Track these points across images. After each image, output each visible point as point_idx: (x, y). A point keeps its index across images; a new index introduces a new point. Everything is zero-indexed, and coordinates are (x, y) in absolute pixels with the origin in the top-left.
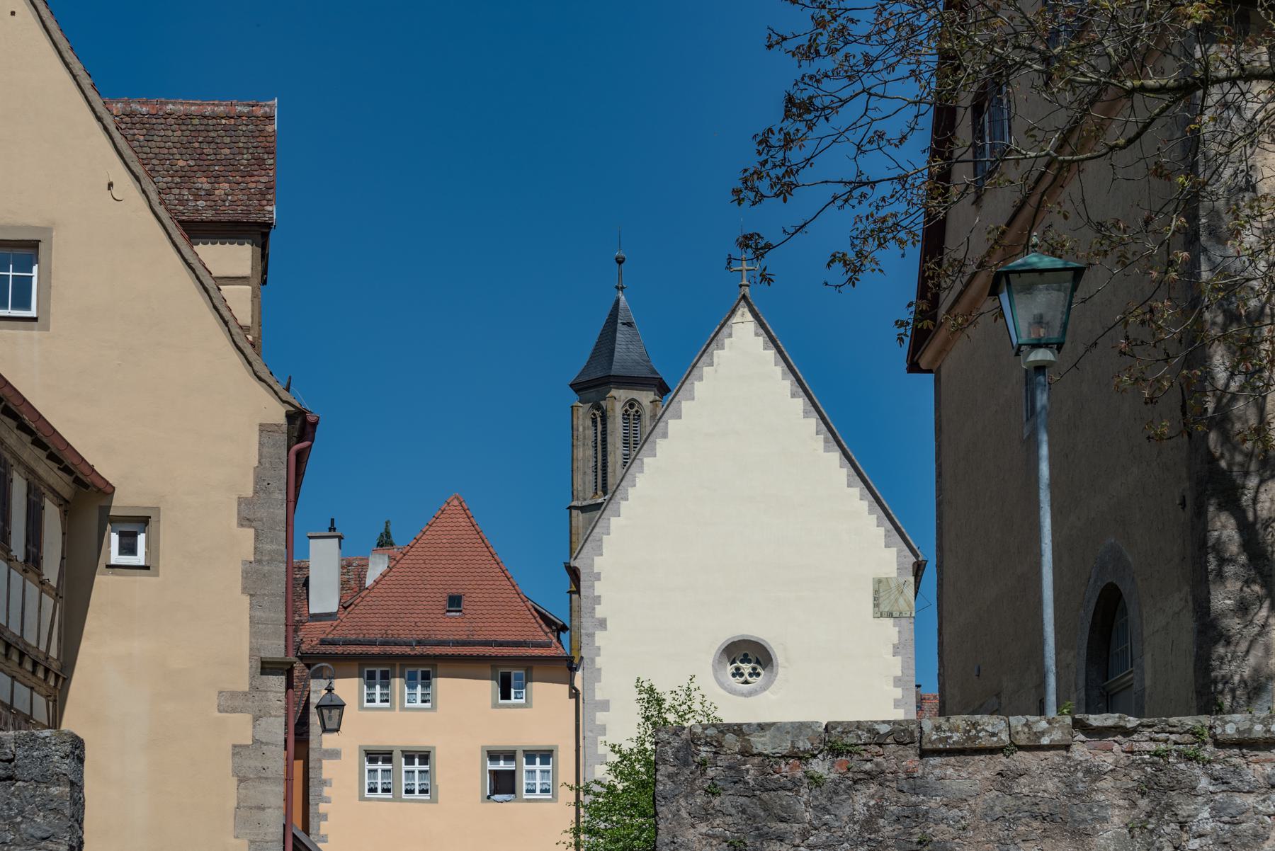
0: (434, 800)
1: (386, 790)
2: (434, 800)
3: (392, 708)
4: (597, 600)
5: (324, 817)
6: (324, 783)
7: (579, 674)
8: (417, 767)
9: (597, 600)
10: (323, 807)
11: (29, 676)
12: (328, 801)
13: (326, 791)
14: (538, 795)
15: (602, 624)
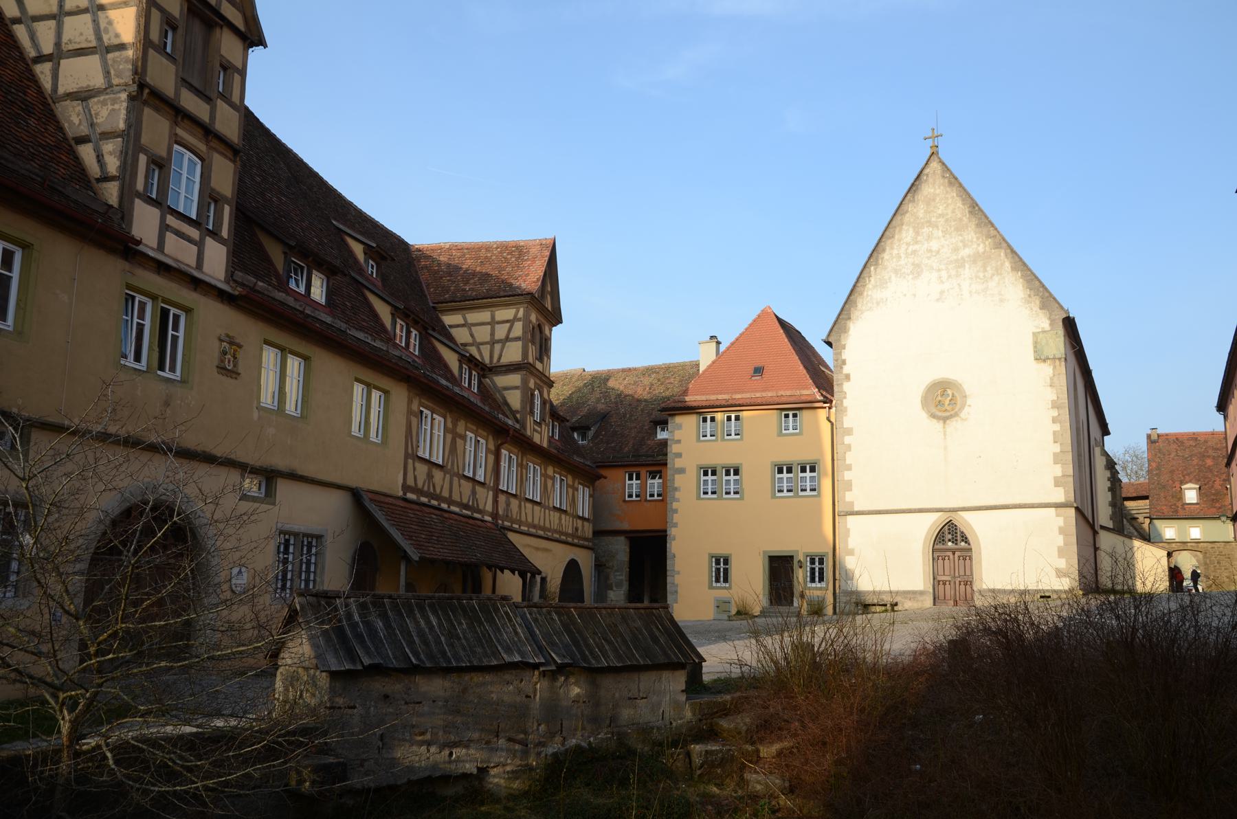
0: (742, 498)
1: (713, 493)
2: (742, 498)
6: (676, 489)
8: (732, 477)
12: (678, 500)
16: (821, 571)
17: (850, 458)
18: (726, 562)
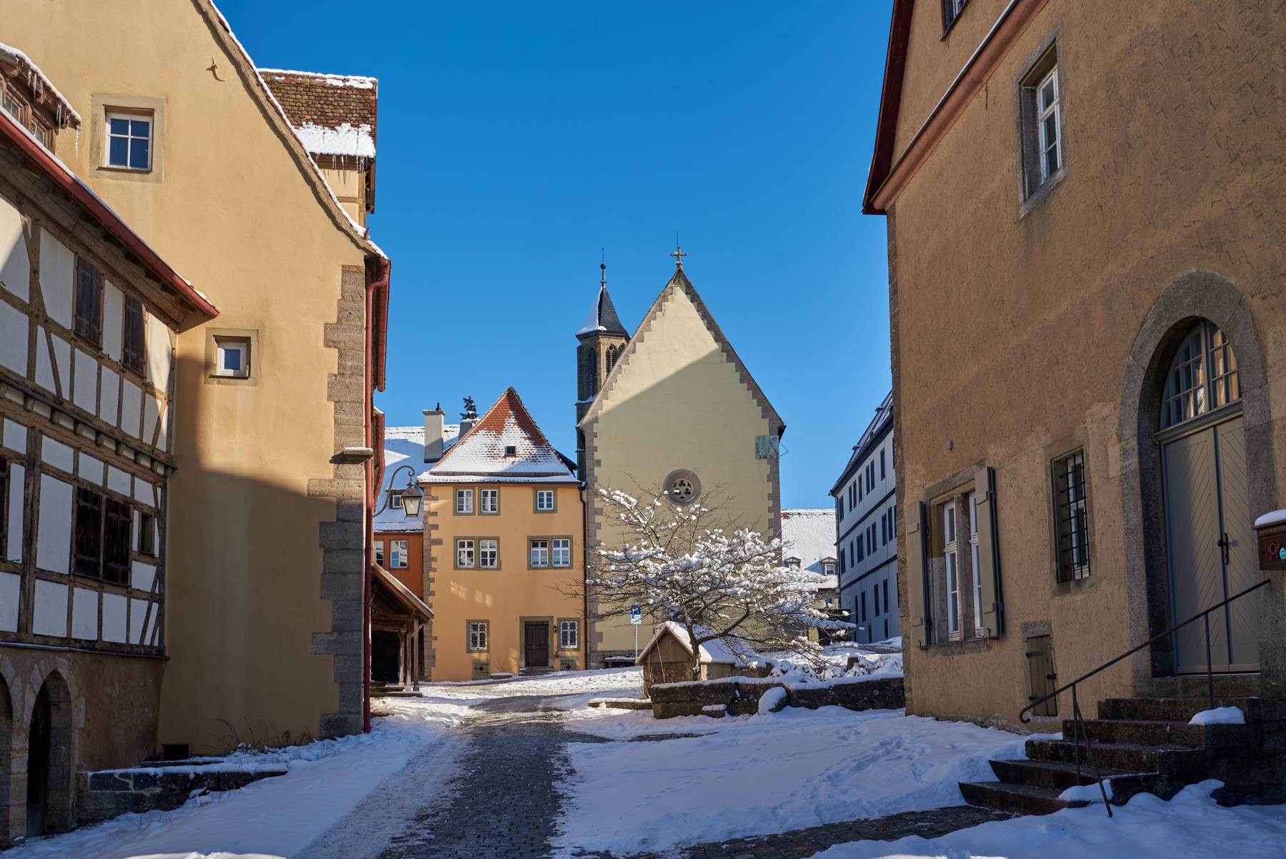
3: (473, 514)
4: (595, 449)
5: (433, 580)
6: (434, 559)
7: (584, 493)
9: (595, 449)
10: (432, 575)
11: (132, 464)
12: (435, 570)
13: (434, 565)
14: (561, 565)
15: (599, 463)
16: (573, 635)
17: (599, 535)
18: (482, 628)
